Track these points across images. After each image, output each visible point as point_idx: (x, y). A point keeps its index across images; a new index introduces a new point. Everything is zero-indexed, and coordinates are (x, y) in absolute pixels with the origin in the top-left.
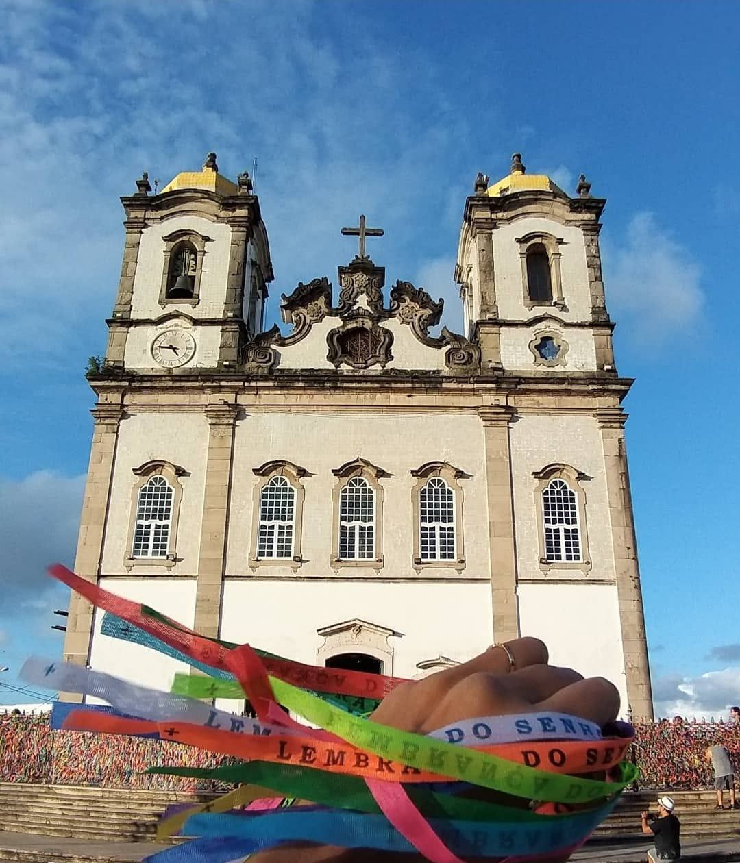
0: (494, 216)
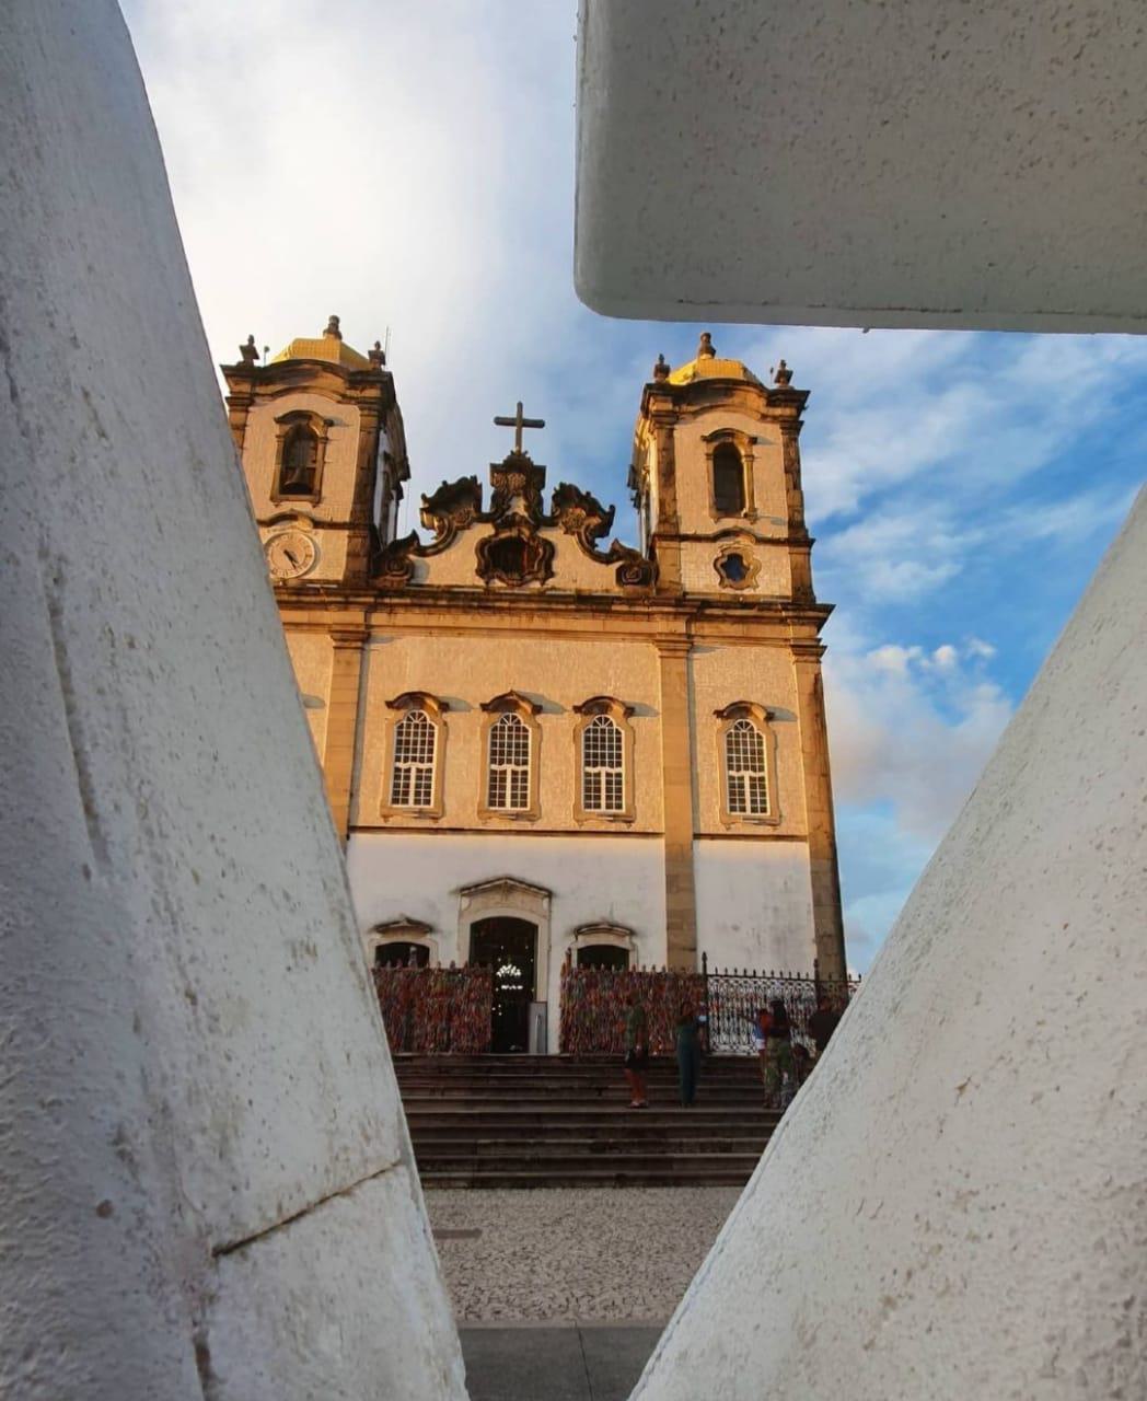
0: (677, 409)
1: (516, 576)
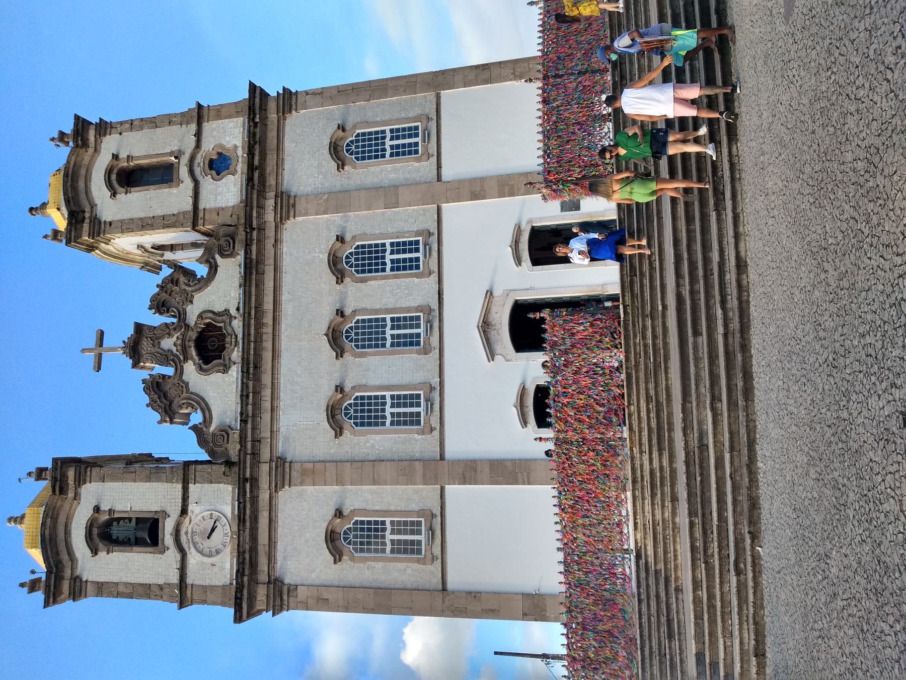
1: (228, 339)
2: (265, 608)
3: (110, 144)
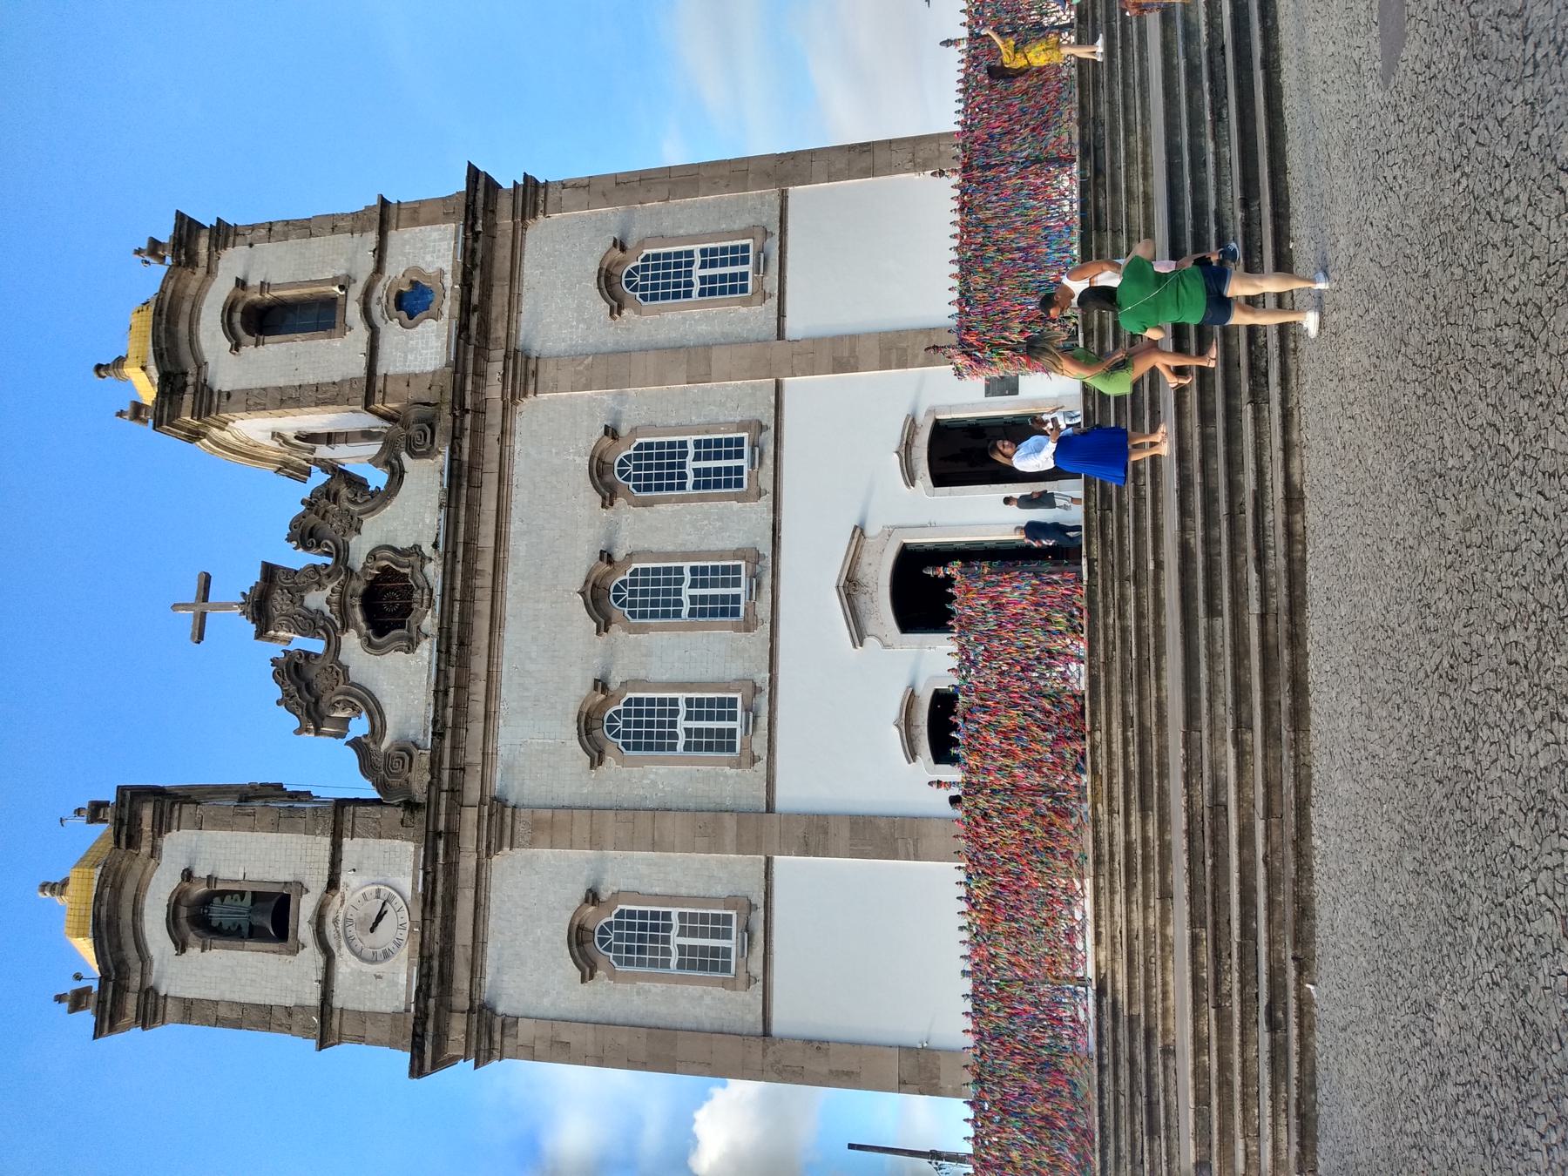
1: (416, 596)
2: (462, 1053)
3: (233, 263)
